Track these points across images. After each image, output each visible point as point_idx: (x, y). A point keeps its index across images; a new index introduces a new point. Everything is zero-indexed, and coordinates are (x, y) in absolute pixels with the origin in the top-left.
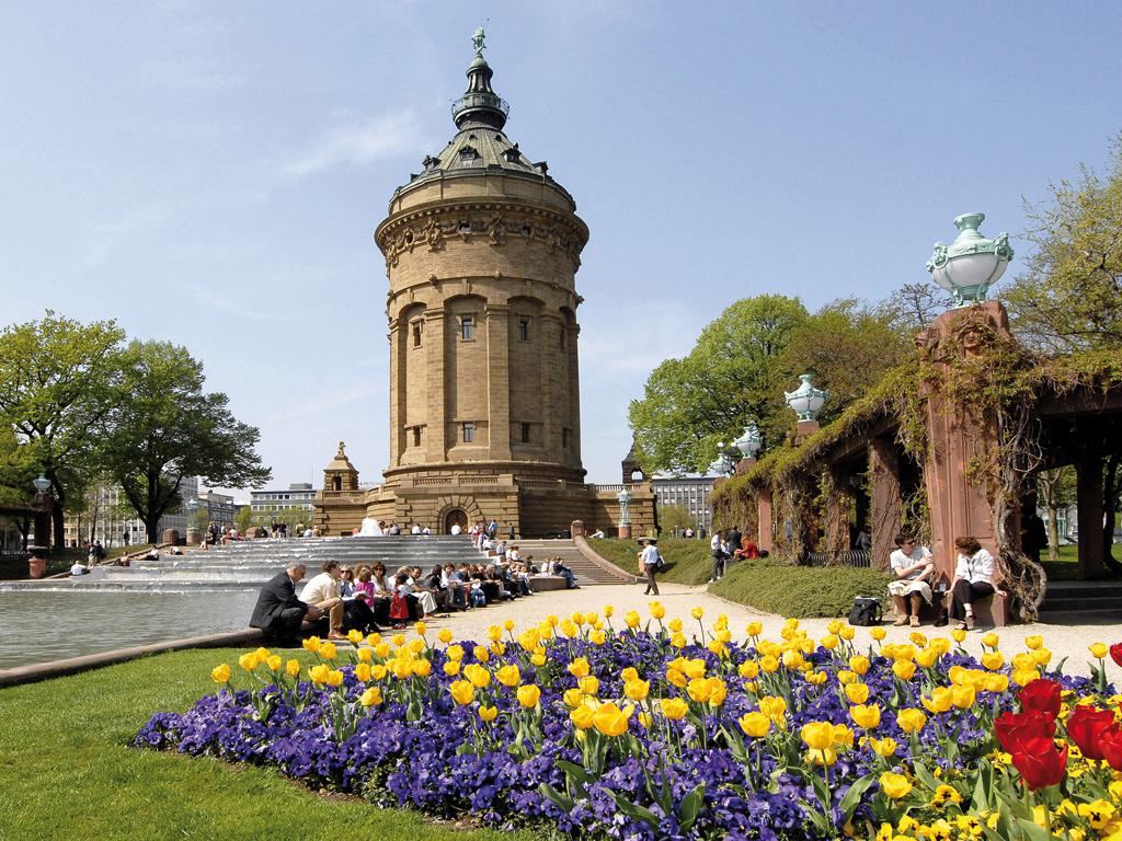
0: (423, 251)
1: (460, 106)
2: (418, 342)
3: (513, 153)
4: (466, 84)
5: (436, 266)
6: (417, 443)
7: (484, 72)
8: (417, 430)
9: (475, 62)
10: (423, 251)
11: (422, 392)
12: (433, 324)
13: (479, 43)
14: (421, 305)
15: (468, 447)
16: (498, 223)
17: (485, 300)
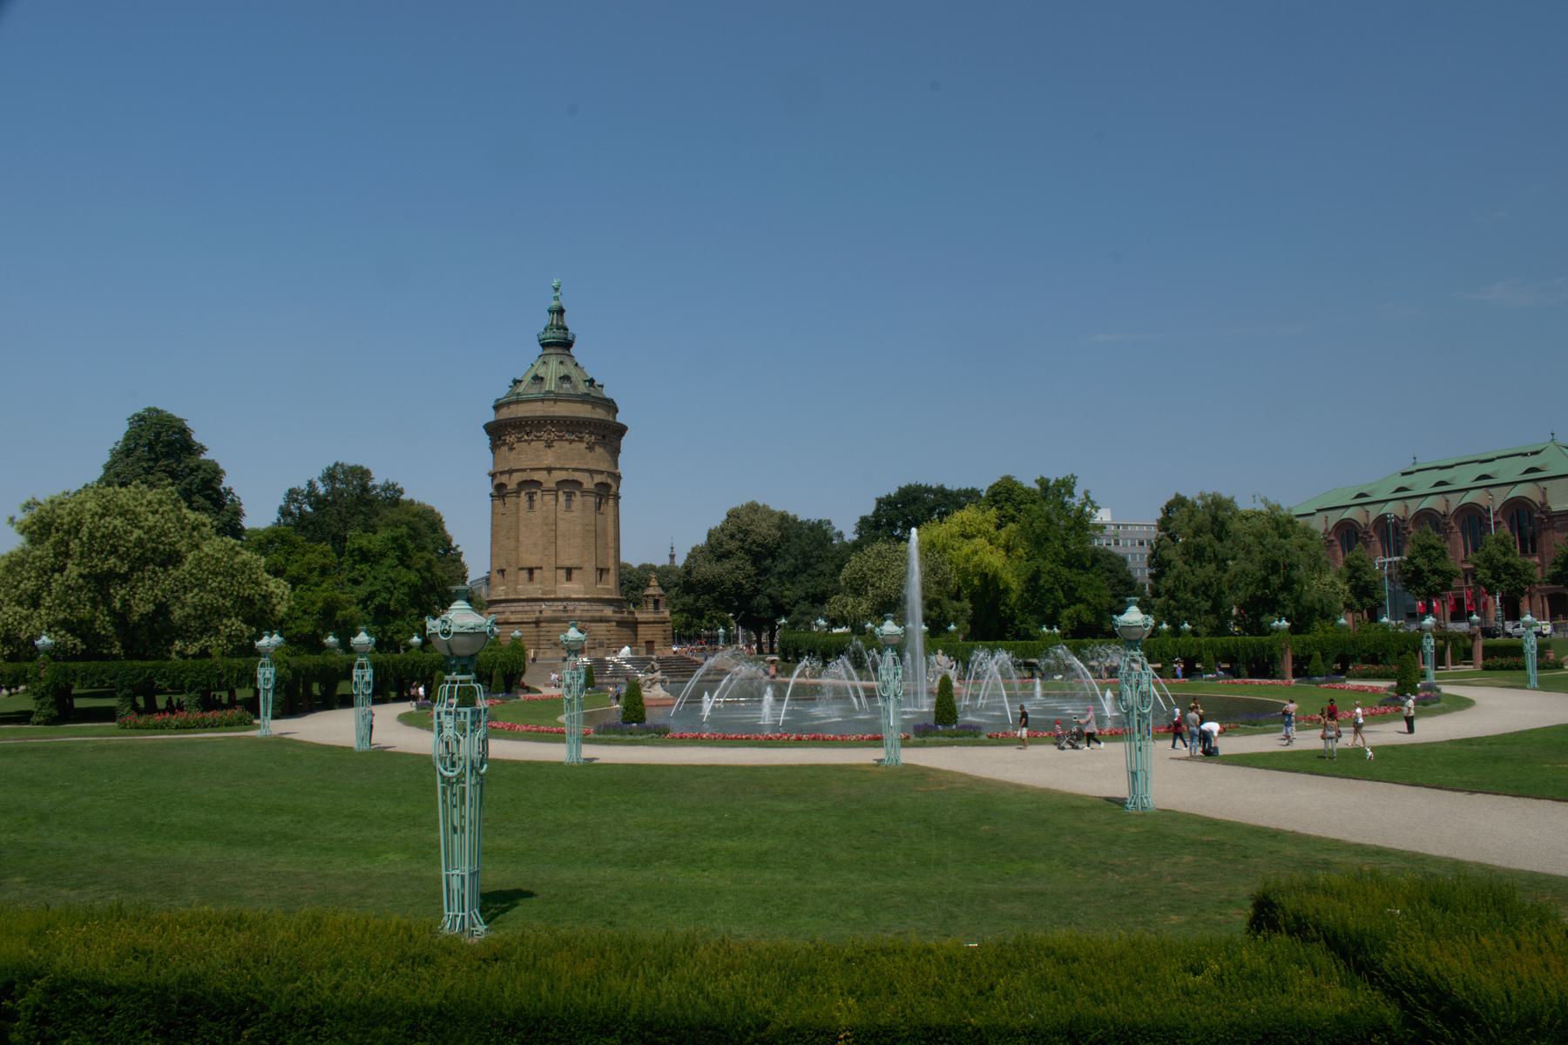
0: (541, 445)
1: (548, 335)
2: (531, 507)
3: (592, 381)
4: (546, 319)
5: (549, 459)
6: (531, 579)
7: (561, 311)
8: (531, 571)
9: (554, 304)
10: (541, 445)
11: (535, 545)
12: (547, 498)
13: (556, 289)
14: (538, 484)
15: (567, 585)
16: (591, 433)
17: (581, 484)
